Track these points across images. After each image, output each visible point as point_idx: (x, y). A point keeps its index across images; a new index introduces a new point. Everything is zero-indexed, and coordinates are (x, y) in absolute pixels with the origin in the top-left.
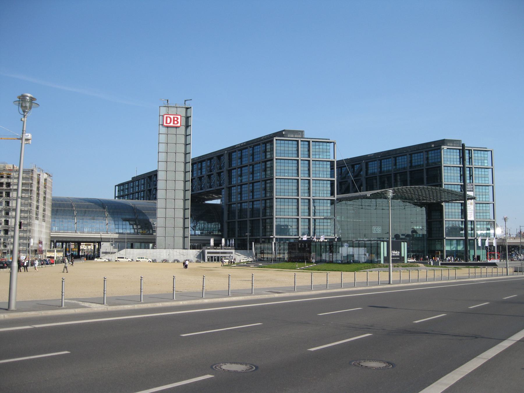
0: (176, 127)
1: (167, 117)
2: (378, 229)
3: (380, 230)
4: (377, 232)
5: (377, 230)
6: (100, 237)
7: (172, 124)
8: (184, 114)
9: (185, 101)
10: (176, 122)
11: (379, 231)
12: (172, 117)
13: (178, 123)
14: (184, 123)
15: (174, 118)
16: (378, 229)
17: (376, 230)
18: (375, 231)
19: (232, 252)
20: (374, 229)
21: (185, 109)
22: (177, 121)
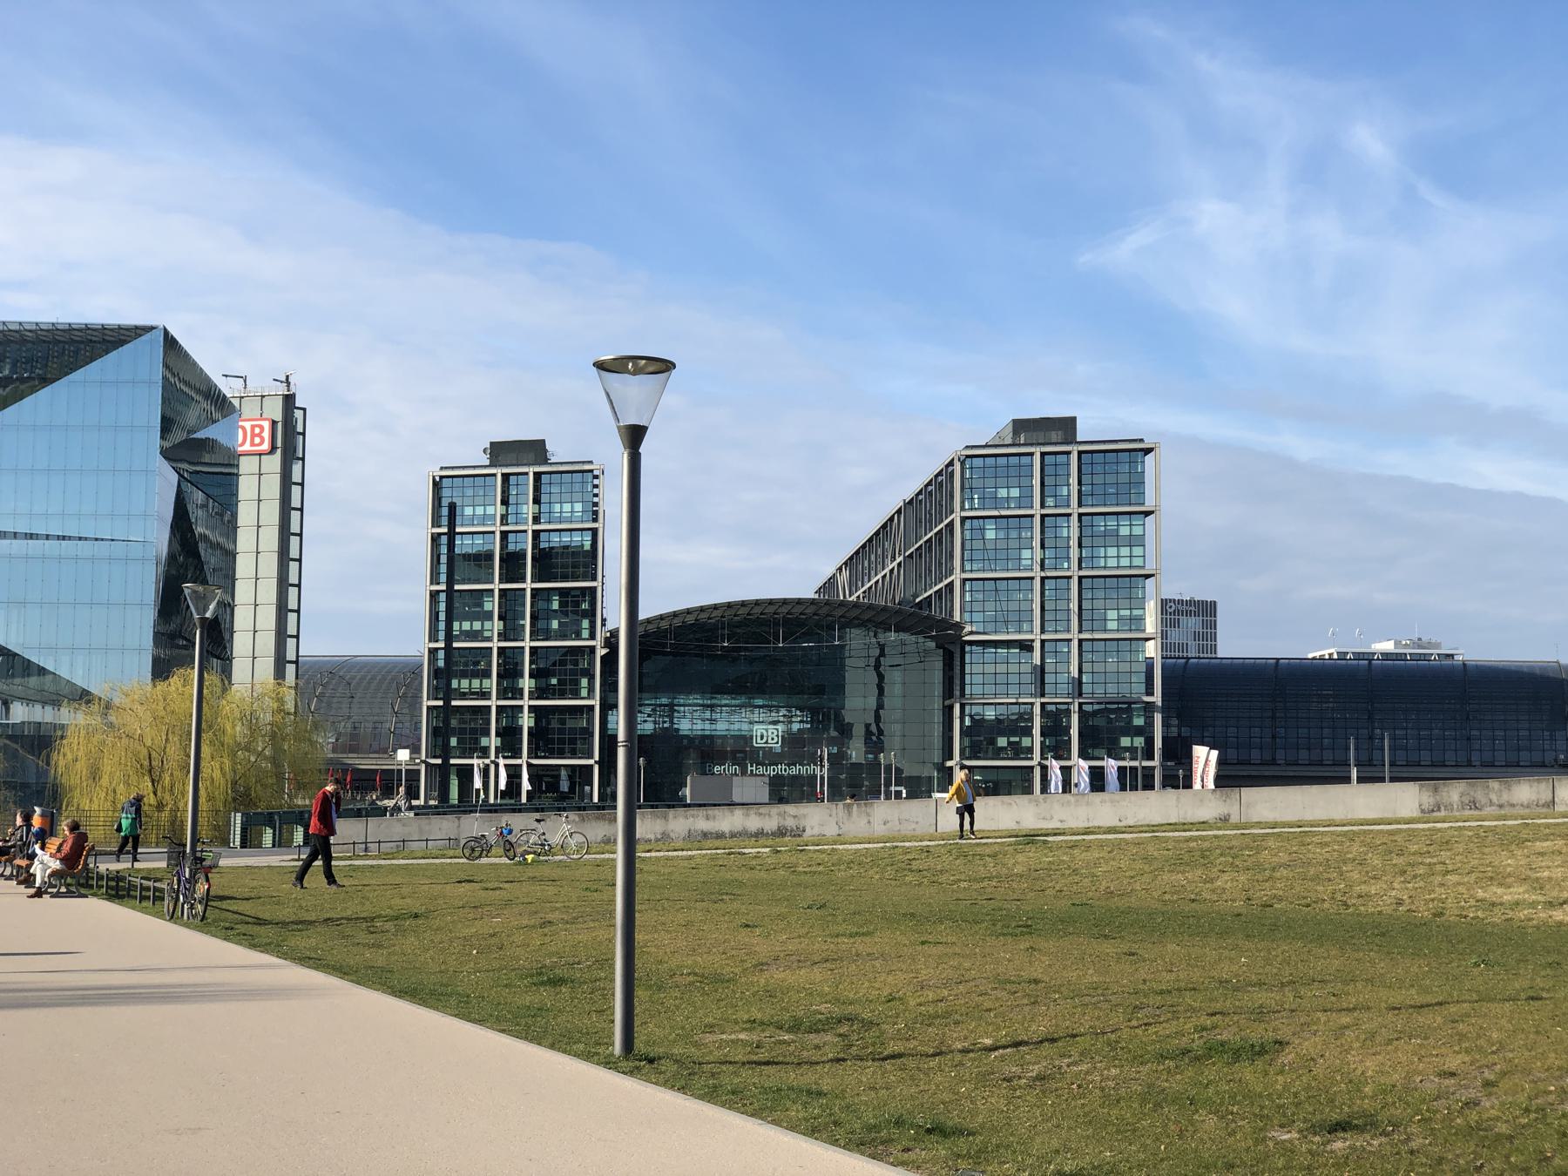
0: (260, 455)
2: (773, 733)
5: (768, 737)
8: (278, 417)
9: (287, 377)
10: (257, 440)
11: (773, 739)
13: (262, 443)
14: (279, 444)
15: (253, 427)
16: (773, 733)
17: (764, 740)
18: (762, 739)
20: (759, 734)
21: (279, 403)
22: (259, 435)
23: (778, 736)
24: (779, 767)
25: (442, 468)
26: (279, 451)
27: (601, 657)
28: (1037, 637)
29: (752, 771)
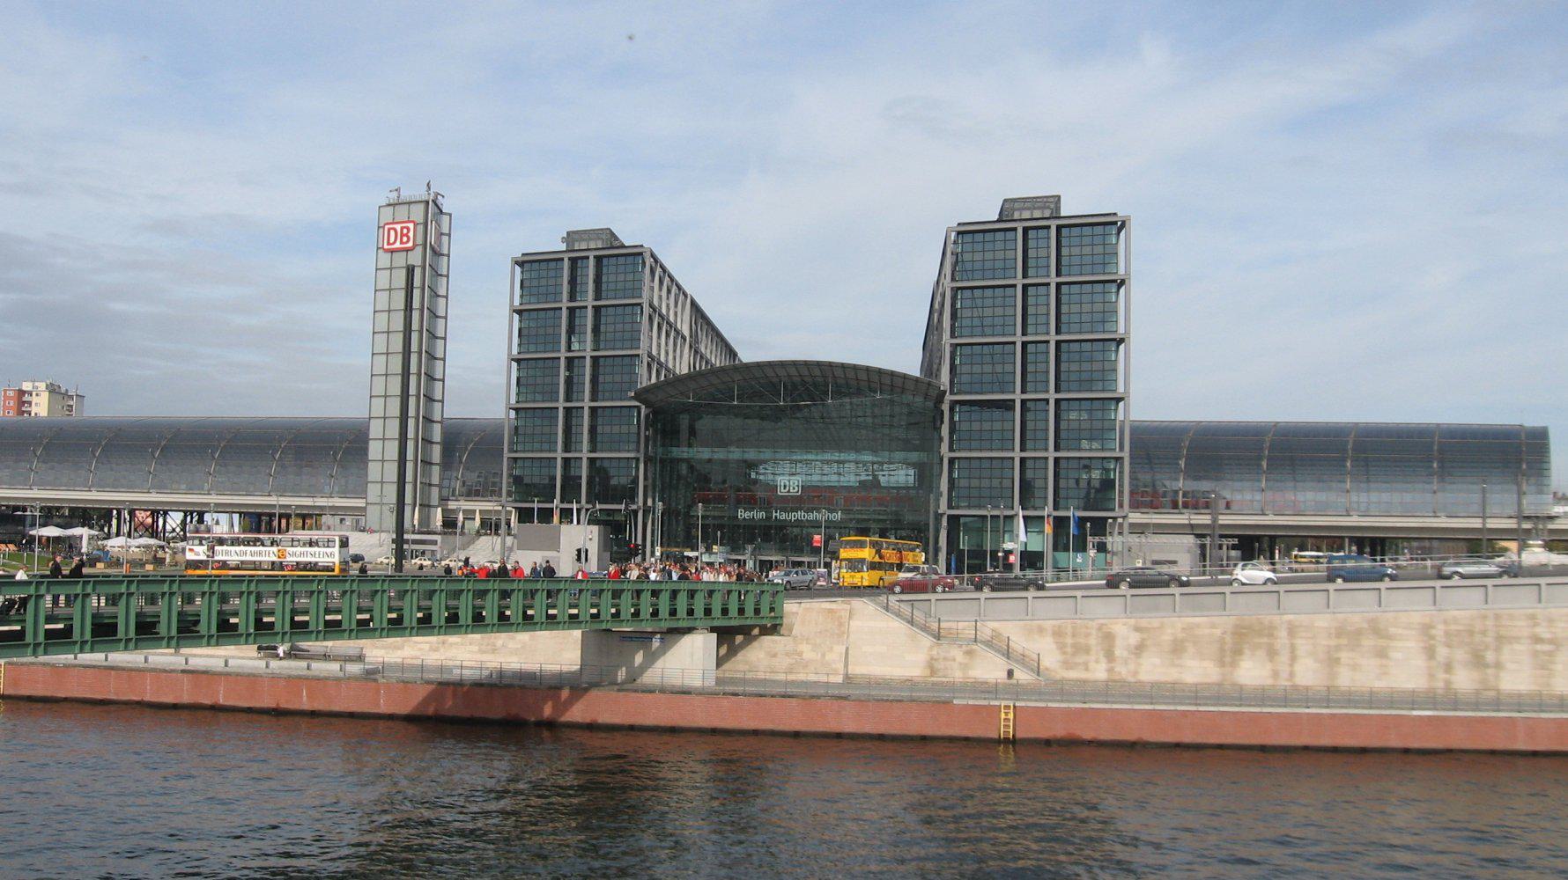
0: (407, 250)
1: (389, 230)
3: (796, 488)
4: (789, 491)
5: (789, 486)
6: (312, 504)
7: (398, 245)
8: (420, 219)
10: (405, 239)
11: (794, 488)
12: (398, 227)
14: (420, 241)
15: (402, 229)
19: (436, 541)
20: (782, 484)
21: (421, 207)
23: (798, 486)
24: (799, 513)
25: (523, 254)
26: (419, 250)
27: (647, 416)
28: (1018, 397)
29: (776, 517)
